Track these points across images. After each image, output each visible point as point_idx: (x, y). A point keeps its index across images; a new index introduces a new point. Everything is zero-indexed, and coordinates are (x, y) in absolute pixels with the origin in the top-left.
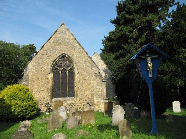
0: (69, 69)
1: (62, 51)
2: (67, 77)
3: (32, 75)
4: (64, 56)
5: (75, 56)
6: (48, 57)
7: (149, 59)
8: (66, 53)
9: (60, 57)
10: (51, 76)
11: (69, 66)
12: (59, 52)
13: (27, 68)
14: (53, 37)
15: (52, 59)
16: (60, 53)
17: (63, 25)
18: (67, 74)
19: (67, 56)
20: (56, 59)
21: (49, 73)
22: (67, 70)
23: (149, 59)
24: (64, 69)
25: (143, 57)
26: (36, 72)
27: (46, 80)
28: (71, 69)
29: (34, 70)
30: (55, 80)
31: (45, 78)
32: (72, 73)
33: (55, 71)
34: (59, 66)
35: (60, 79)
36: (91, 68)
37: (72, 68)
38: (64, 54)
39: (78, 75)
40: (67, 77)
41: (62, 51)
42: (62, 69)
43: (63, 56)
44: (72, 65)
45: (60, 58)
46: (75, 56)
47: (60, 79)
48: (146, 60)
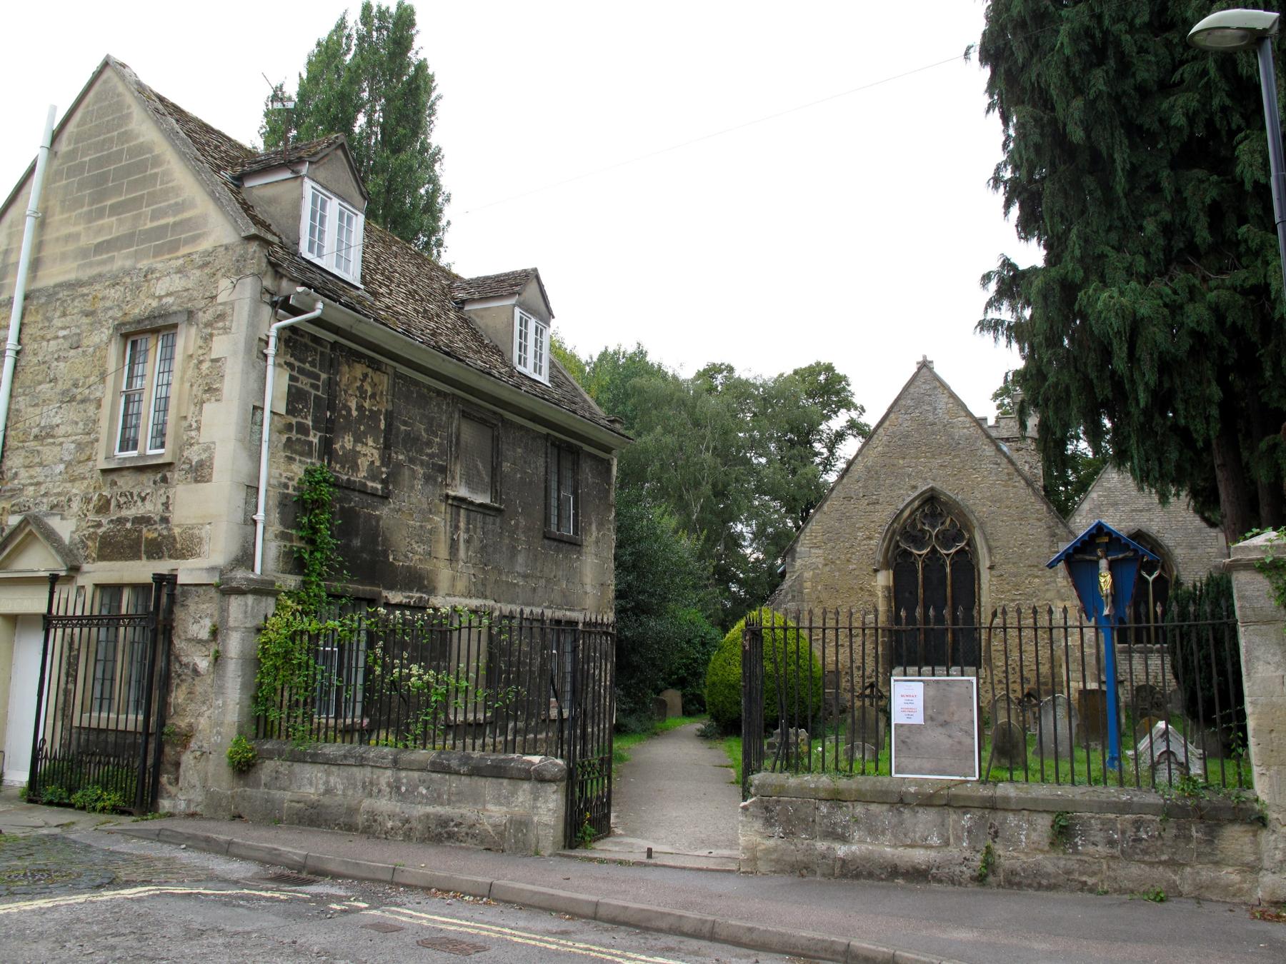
0: (953, 551)
1: (925, 479)
2: (949, 582)
3: (816, 576)
4: (932, 503)
5: (979, 496)
6: (869, 508)
7: (1103, 563)
8: (938, 485)
9: (916, 503)
10: (883, 579)
11: (958, 537)
12: (913, 483)
13: (795, 551)
14: (887, 423)
15: (884, 516)
16: (914, 487)
17: (924, 370)
18: (948, 570)
19: (943, 498)
20: (902, 511)
21: (876, 571)
22: (948, 555)
23: (1103, 563)
24: (934, 550)
25: (1088, 557)
26: (827, 568)
27: (866, 598)
28: (961, 551)
29: (821, 560)
30: (900, 594)
31: (861, 589)
32: (966, 566)
33: (898, 561)
34: (919, 540)
35: (920, 591)
36: (1047, 544)
37: (968, 544)
38: (932, 489)
39: (992, 576)
40: (949, 582)
41: (925, 479)
42: (925, 552)
43: (932, 503)
44: (967, 536)
45: (917, 509)
46: (979, 496)
47: (920, 591)
48: (1097, 563)
